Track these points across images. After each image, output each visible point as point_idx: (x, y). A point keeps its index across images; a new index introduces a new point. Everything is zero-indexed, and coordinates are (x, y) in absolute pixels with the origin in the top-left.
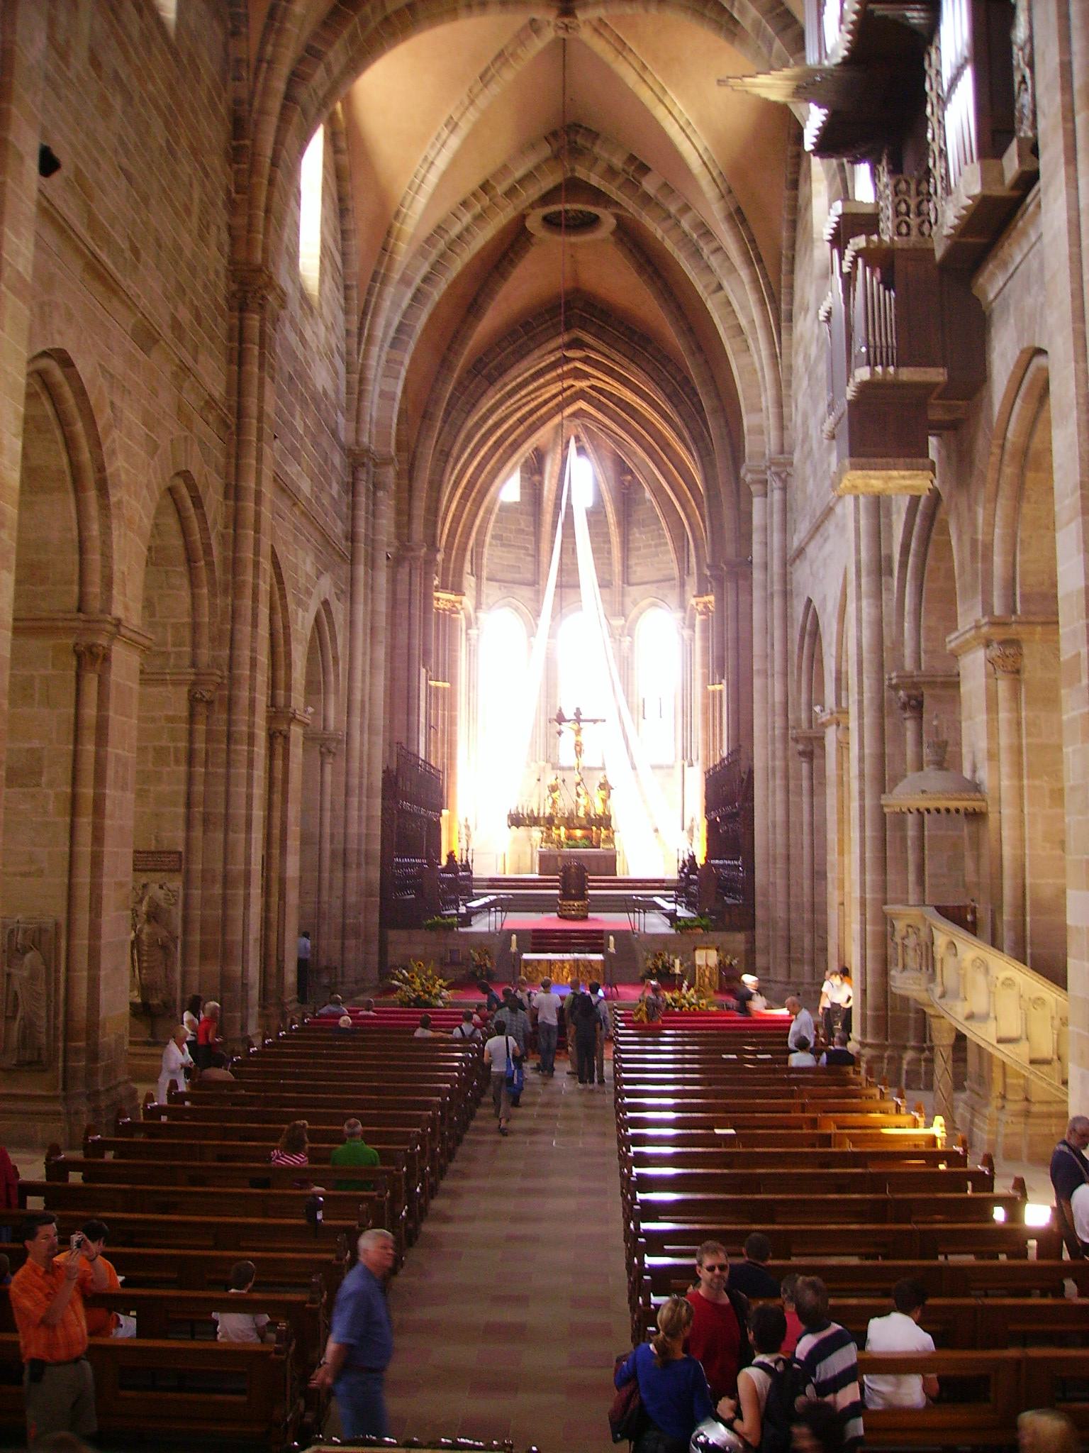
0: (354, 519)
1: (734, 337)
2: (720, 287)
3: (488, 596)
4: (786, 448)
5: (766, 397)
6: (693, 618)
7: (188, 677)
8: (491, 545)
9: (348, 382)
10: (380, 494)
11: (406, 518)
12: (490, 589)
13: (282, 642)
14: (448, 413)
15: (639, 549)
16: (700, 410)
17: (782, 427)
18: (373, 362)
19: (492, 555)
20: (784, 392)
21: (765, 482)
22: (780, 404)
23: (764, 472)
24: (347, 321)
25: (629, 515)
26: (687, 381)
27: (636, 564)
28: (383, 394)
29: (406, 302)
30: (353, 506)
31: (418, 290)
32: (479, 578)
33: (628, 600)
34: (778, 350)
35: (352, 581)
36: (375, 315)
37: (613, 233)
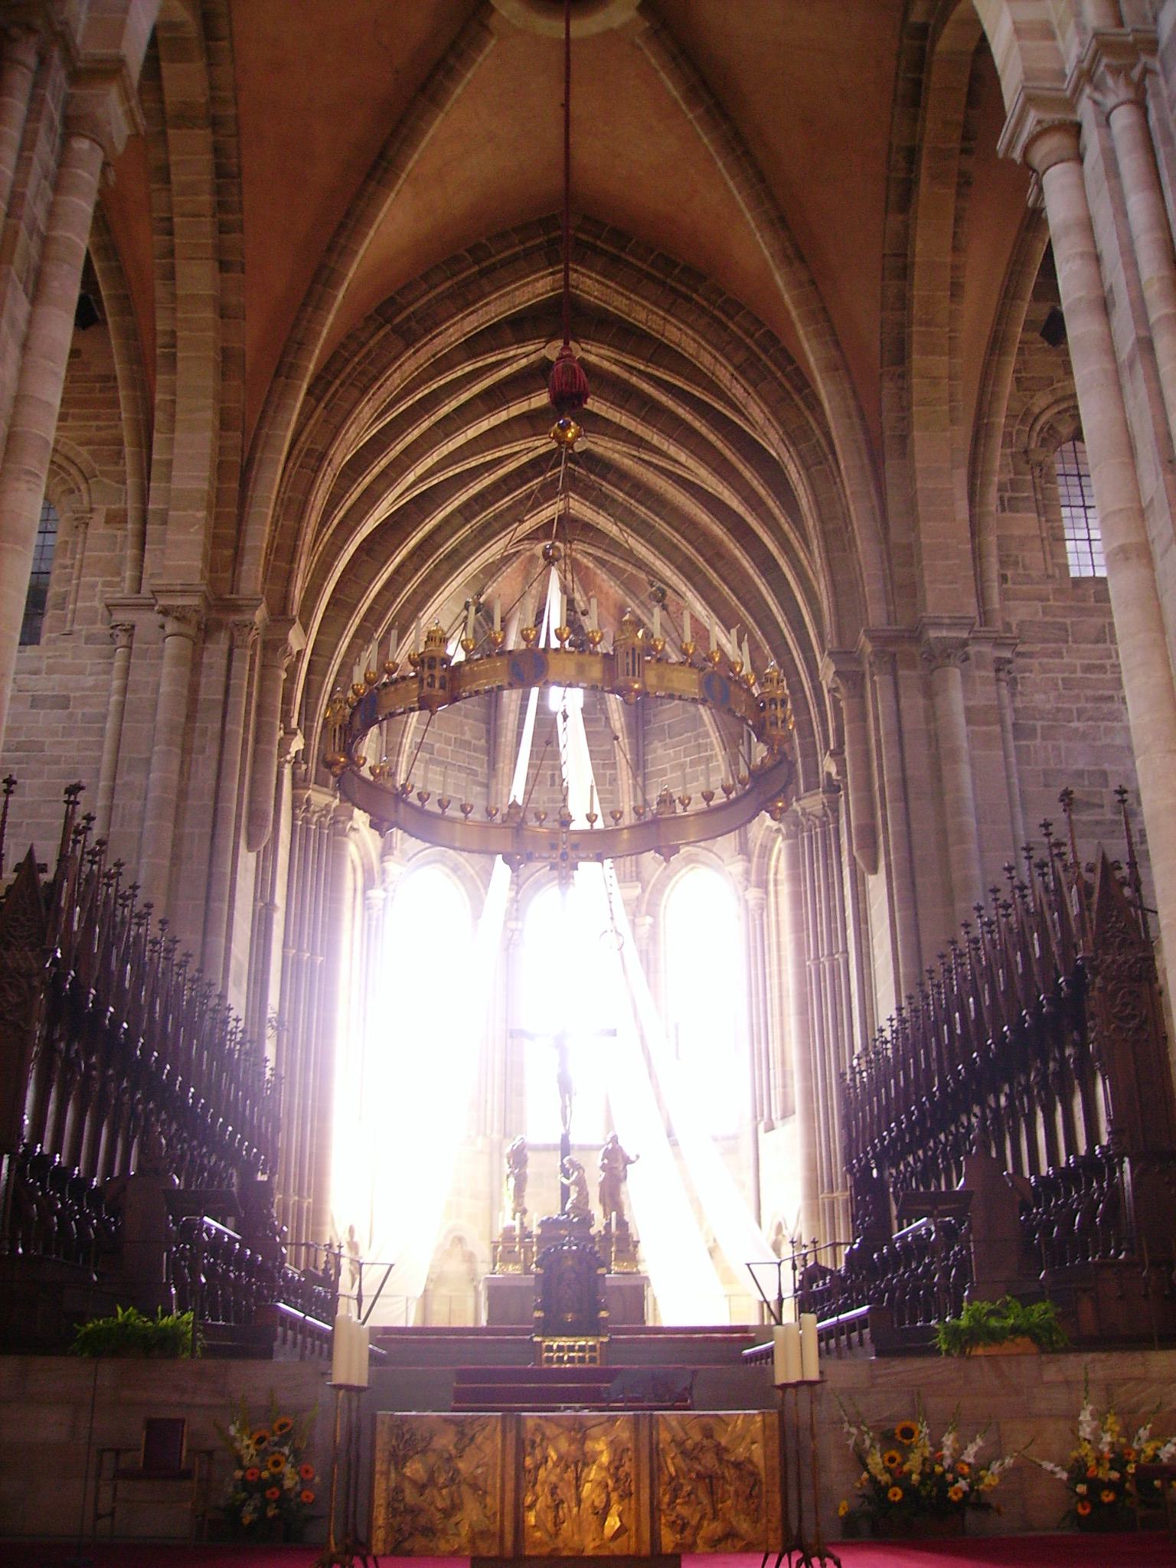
6: (763, 870)
10: (82, 145)
11: (228, 552)
23: (1071, 104)
25: (647, 722)
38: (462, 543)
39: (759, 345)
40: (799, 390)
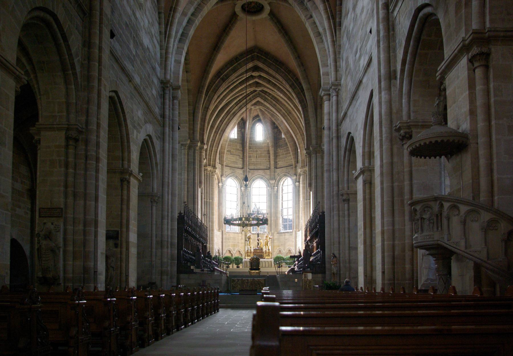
0: (164, 108)
1: (317, 37)
2: (311, 17)
3: (226, 172)
4: (338, 79)
5: (330, 59)
7: (64, 126)
8: (227, 154)
9: (161, 54)
10: (175, 101)
11: (192, 132)
12: (227, 170)
13: (126, 141)
14: (207, 92)
15: (280, 156)
16: (302, 90)
17: (336, 70)
18: (171, 45)
19: (227, 158)
20: (337, 56)
21: (329, 95)
22: (335, 61)
23: (329, 90)
24: (160, 28)
25: (277, 144)
26: (297, 79)
27: (279, 161)
28: (176, 61)
29: (184, 24)
30: (164, 104)
31: (190, 19)
32: (222, 165)
33: (276, 174)
34: (335, 39)
35: (163, 134)
36: (171, 25)
37: (269, 14)
38: (236, 110)
39: (294, 81)
40: (302, 92)
